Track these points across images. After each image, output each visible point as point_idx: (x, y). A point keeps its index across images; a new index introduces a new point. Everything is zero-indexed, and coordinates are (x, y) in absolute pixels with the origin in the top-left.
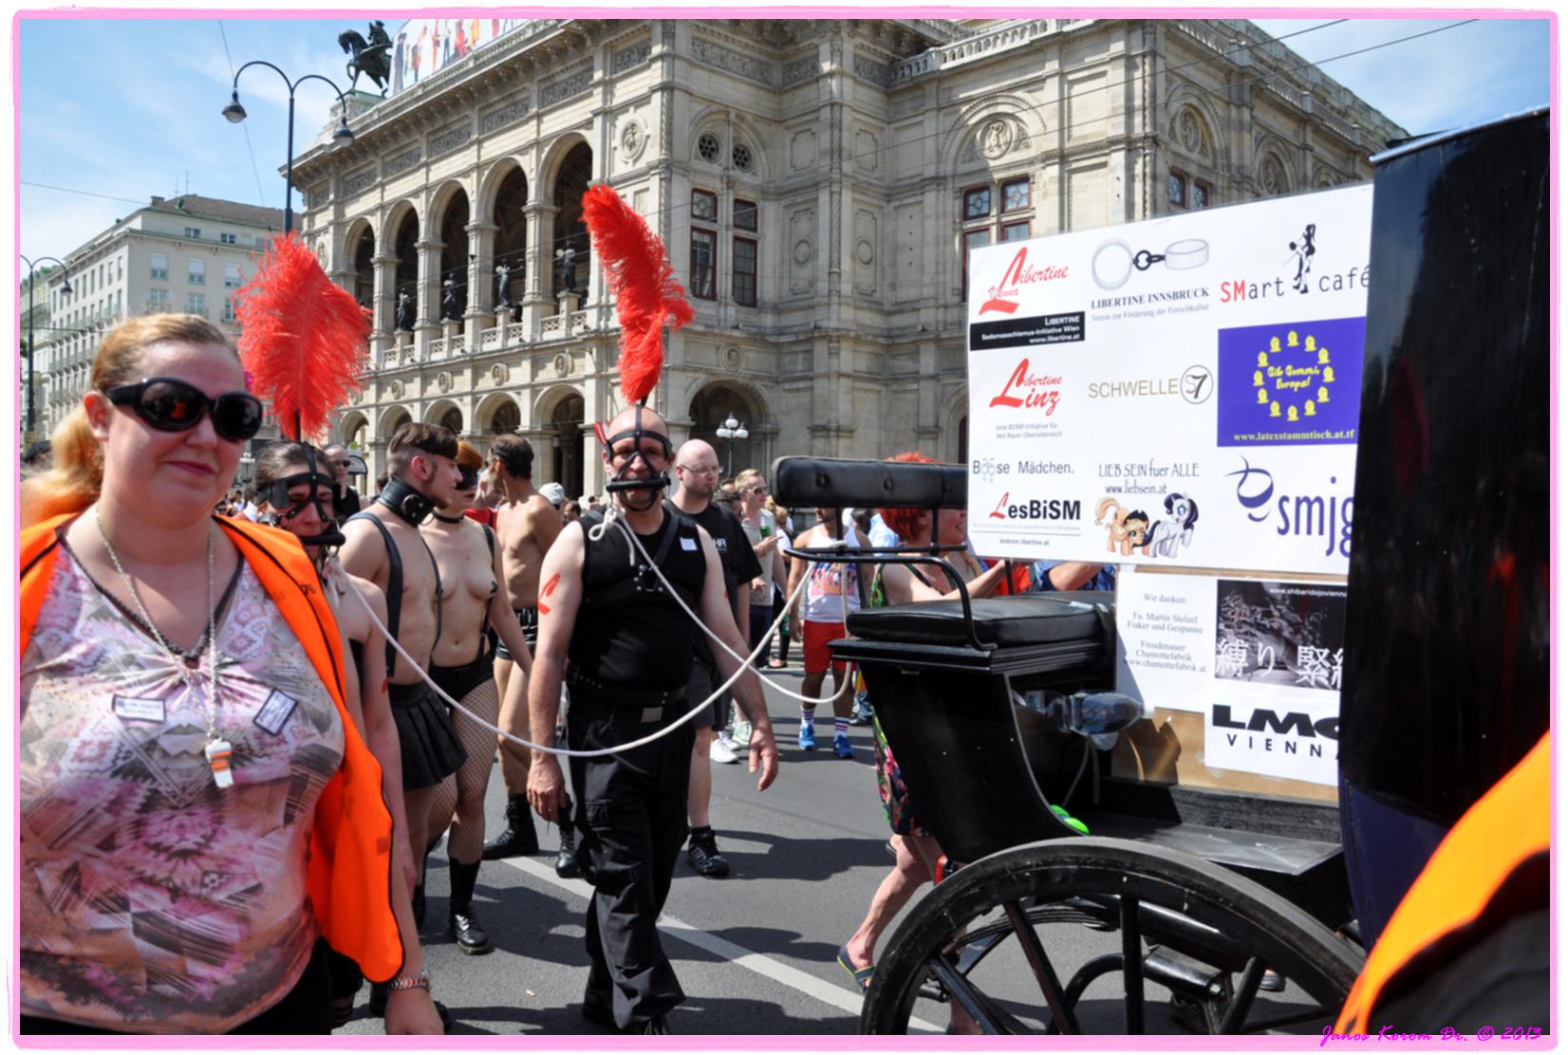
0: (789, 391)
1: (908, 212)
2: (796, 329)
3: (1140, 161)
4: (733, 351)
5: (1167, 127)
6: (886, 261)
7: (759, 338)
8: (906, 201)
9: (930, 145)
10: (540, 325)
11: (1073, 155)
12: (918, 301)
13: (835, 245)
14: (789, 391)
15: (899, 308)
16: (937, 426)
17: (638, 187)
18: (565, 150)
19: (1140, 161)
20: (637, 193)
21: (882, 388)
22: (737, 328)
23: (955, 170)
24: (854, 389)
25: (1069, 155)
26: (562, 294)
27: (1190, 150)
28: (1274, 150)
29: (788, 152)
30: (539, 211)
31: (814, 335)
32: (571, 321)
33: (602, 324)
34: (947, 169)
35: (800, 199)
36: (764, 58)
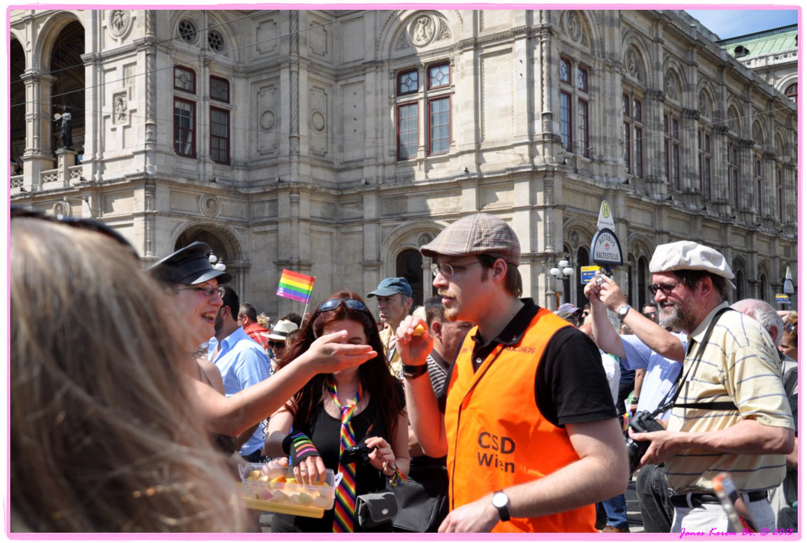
0: (258, 233)
1: (352, 89)
2: (263, 183)
3: (538, 47)
4: (211, 200)
5: (558, 21)
6: (335, 129)
7: (232, 190)
8: (351, 81)
9: (370, 37)
10: (40, 176)
11: (484, 43)
12: (361, 160)
13: (294, 115)
14: (258, 233)
15: (347, 166)
16: (378, 260)
18: (59, 27)
19: (538, 47)
20: (125, 66)
21: (334, 231)
22: (214, 181)
23: (390, 55)
24: (311, 231)
25: (482, 43)
26: (60, 151)
27: (575, 40)
28: (635, 42)
29: (254, 38)
30: (35, 78)
31: (278, 187)
32: (69, 174)
33: (97, 177)
34: (384, 55)
35: (264, 77)
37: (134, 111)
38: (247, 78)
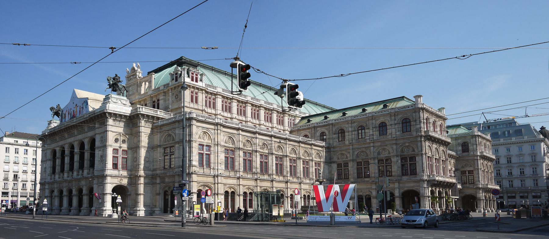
1: (155, 151)
12: (156, 169)
17: (103, 149)
20: (103, 150)
28: (230, 136)
34: (162, 144)
35: (134, 150)
36: (128, 123)
37: (104, 160)
38: (131, 150)
